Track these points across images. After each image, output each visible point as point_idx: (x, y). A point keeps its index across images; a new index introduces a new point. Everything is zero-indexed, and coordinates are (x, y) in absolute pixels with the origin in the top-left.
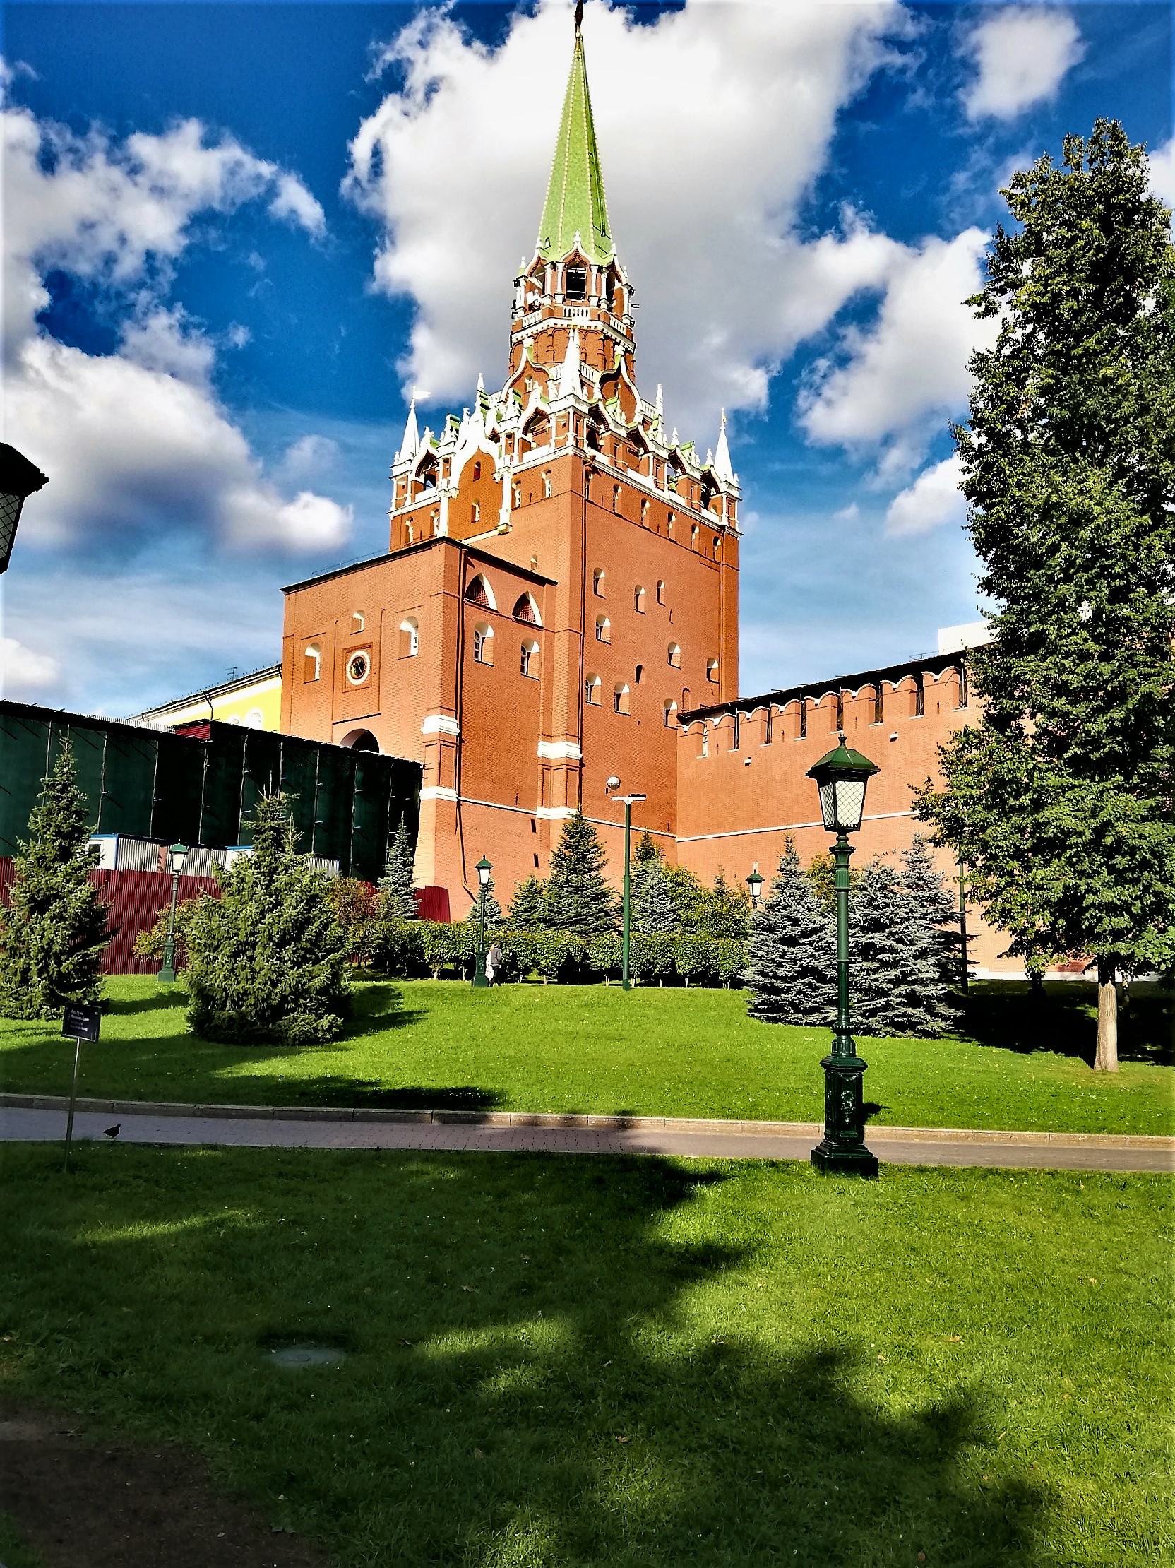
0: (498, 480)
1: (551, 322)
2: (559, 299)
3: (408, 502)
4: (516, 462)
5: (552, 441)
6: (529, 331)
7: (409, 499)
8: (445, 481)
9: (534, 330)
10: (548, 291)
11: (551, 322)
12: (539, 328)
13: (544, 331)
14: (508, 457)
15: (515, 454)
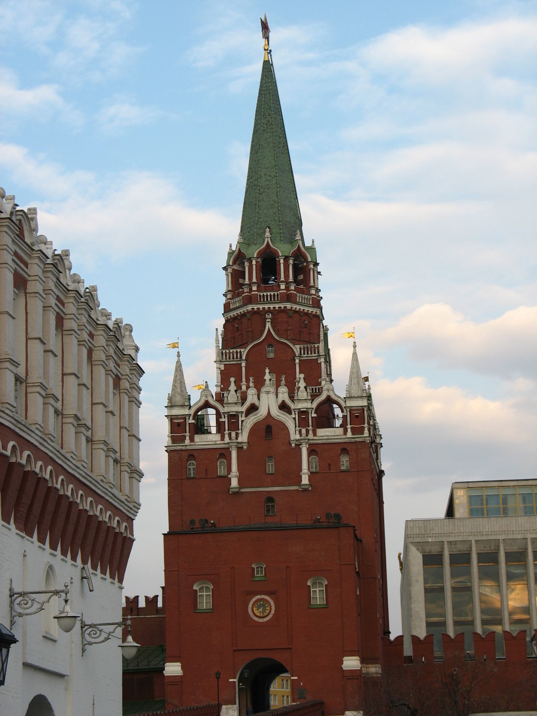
0: (293, 445)
1: (289, 306)
2: (292, 288)
3: (187, 441)
4: (311, 436)
5: (349, 426)
6: (266, 307)
7: (188, 438)
8: (233, 434)
9: (272, 306)
10: (282, 278)
11: (289, 306)
12: (277, 306)
13: (280, 310)
14: (304, 431)
15: (310, 428)
